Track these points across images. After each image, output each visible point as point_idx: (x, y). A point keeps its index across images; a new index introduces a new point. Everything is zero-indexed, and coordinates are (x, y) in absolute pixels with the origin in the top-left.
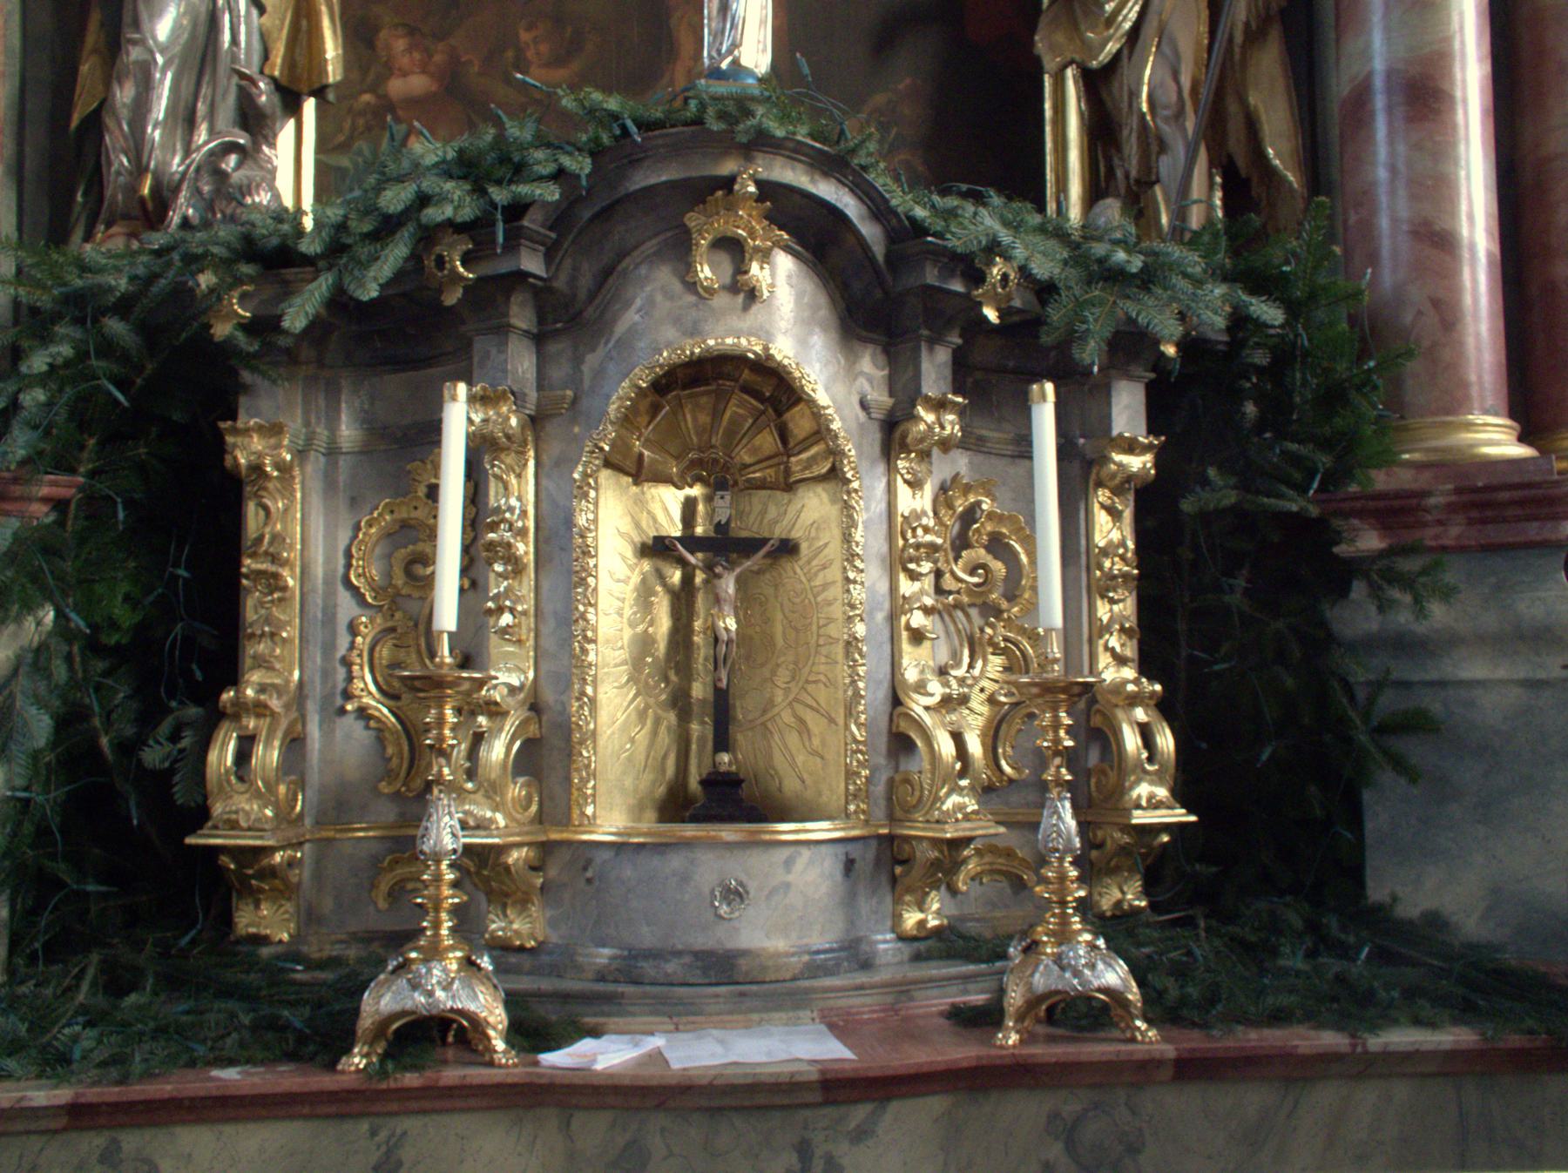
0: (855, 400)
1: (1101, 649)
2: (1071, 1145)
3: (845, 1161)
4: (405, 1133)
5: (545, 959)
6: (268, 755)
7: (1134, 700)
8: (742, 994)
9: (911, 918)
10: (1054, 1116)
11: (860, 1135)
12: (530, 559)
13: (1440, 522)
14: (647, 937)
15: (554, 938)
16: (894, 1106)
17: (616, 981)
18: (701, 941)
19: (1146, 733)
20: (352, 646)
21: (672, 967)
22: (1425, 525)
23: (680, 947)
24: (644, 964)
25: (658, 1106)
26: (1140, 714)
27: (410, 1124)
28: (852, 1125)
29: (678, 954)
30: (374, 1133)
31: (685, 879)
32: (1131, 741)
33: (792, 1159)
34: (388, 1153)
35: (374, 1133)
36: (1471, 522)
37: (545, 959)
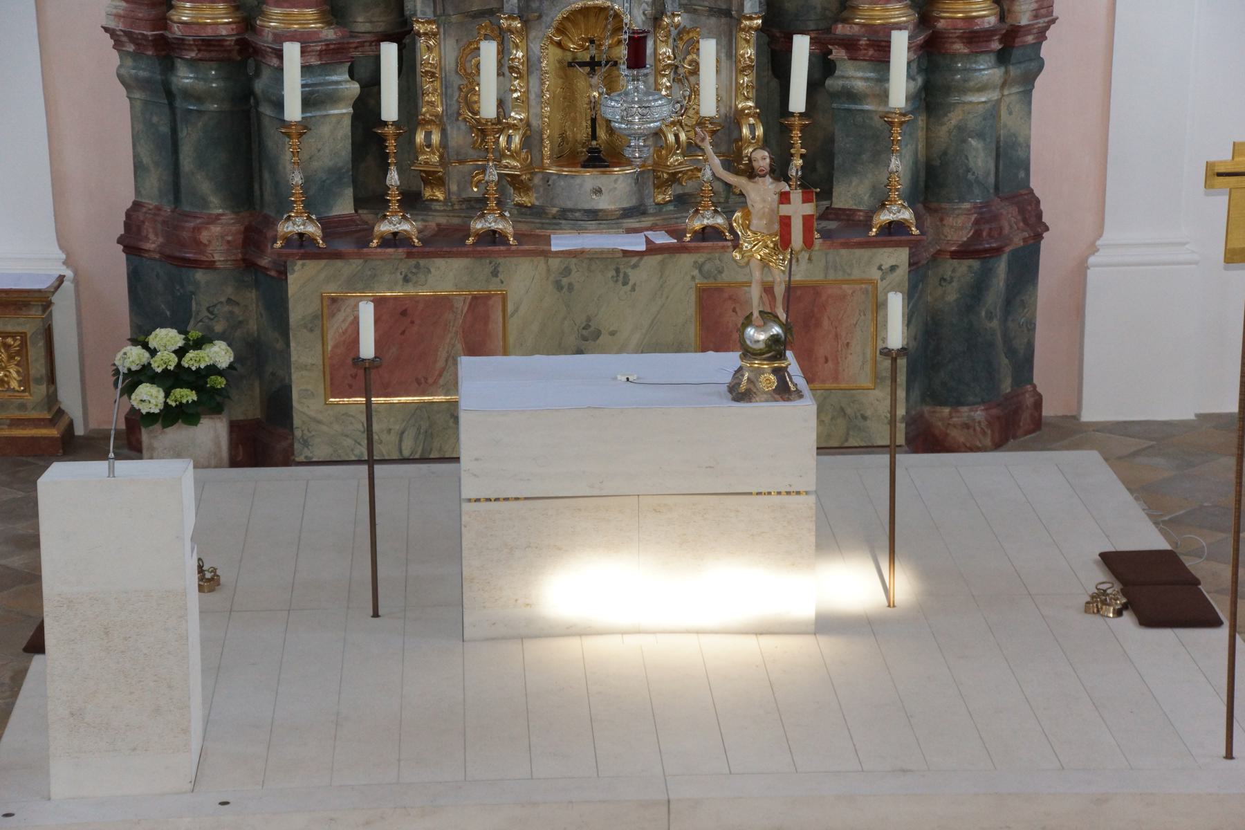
0: (641, 12)
1: (739, 94)
2: (700, 271)
3: (630, 274)
4: (499, 264)
5: (535, 210)
6: (436, 138)
7: (749, 115)
8: (600, 224)
9: (660, 198)
10: (695, 262)
11: (635, 266)
12: (525, 73)
13: (865, 50)
14: (570, 205)
15: (537, 203)
16: (646, 258)
17: (559, 219)
18: (587, 207)
19: (752, 128)
20: (459, 96)
21: (577, 214)
22: (861, 50)
23: (580, 208)
24: (568, 213)
25: (574, 257)
26: (752, 120)
27: (500, 260)
28: (632, 264)
29: (579, 210)
30: (490, 263)
31: (581, 186)
32: (745, 131)
33: (614, 273)
34: (495, 269)
35: (490, 263)
36: (875, 51)
37: (535, 210)
